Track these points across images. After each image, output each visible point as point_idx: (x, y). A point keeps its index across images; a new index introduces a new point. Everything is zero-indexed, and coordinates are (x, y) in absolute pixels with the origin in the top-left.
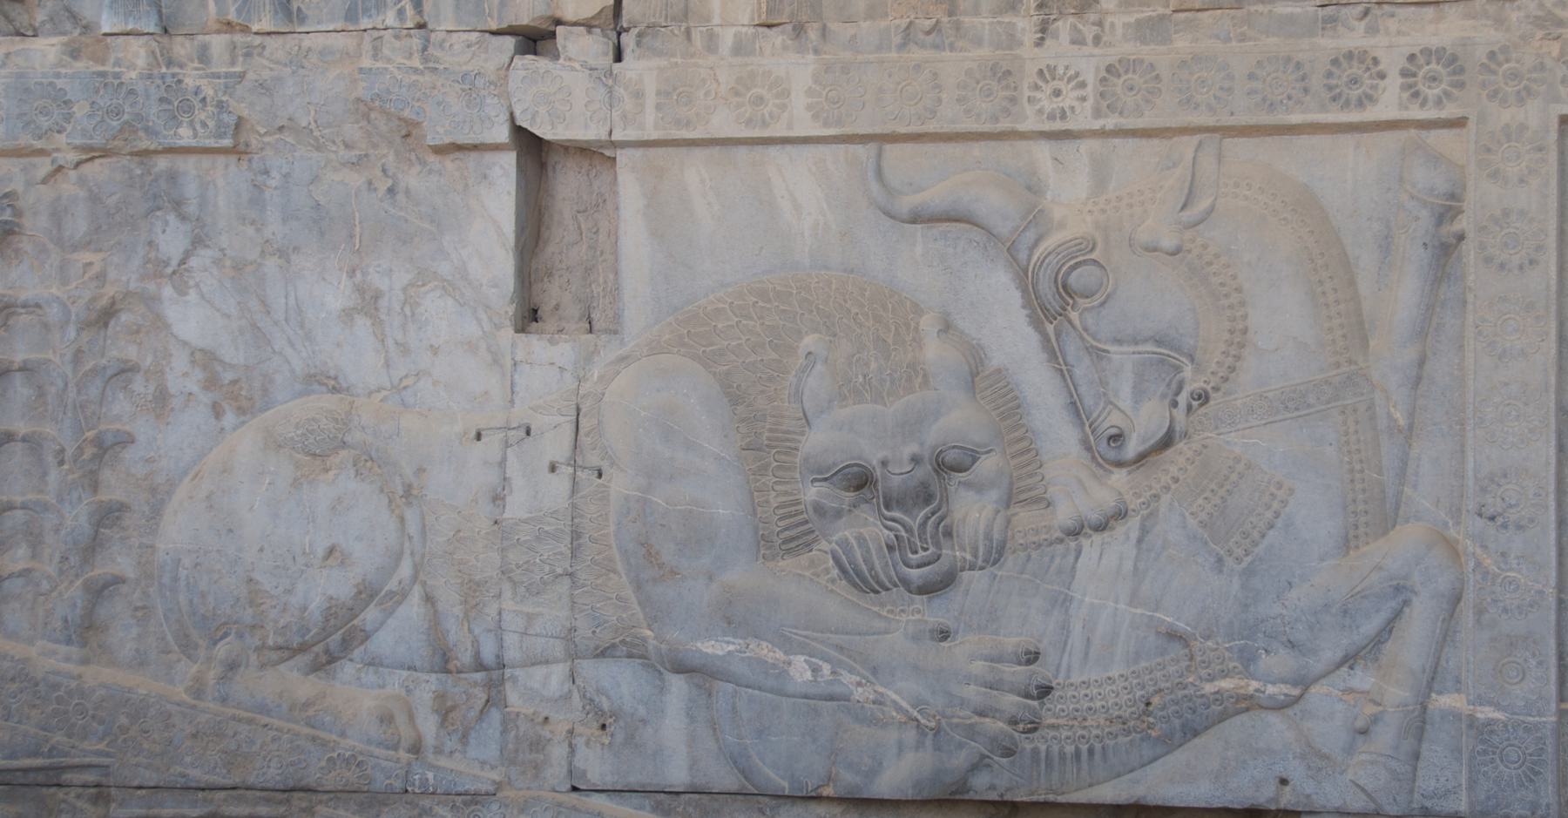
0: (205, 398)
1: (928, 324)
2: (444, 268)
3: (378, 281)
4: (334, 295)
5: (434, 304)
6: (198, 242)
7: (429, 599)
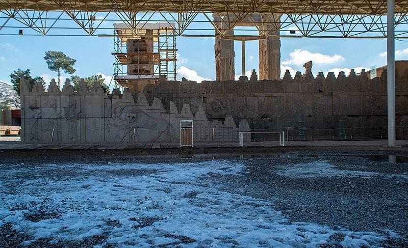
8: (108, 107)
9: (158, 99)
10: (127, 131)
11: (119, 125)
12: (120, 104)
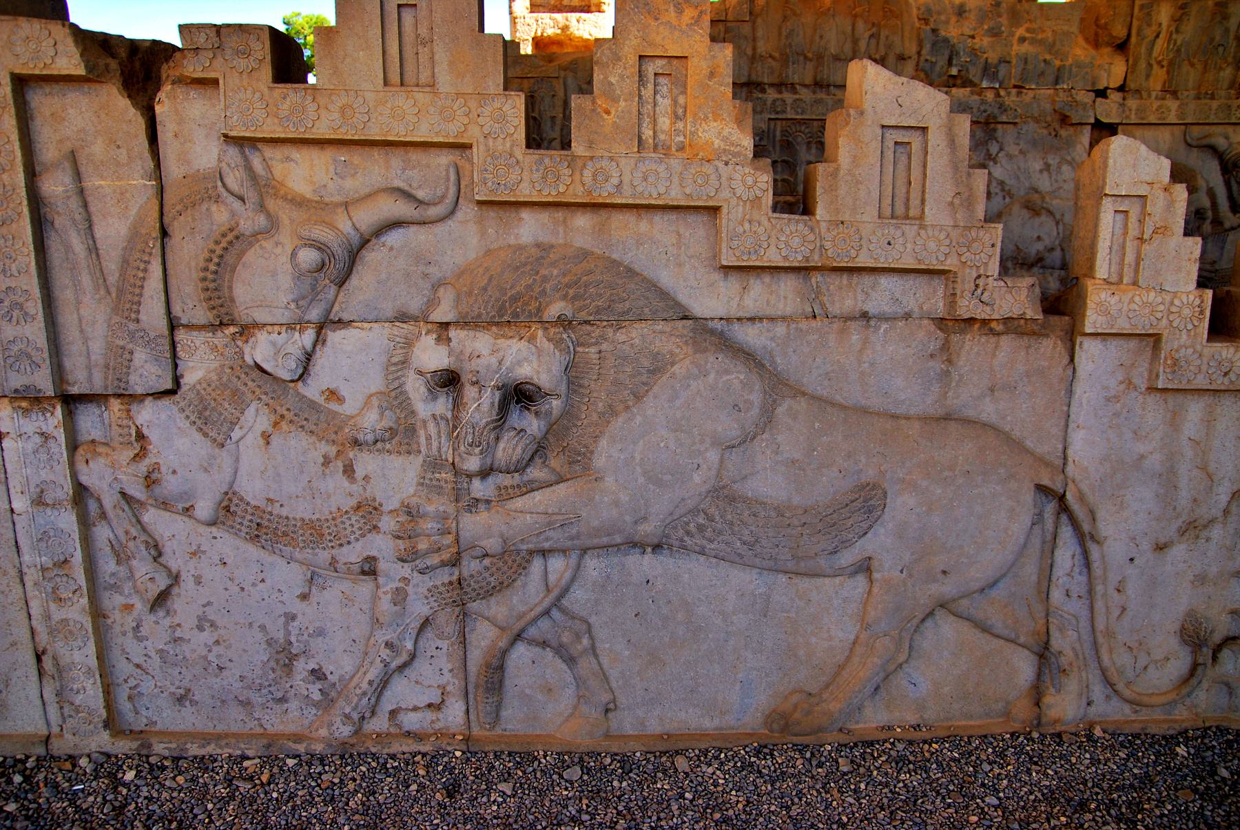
0: (1001, 194)
1: (1199, 177)
2: (1069, 158)
3: (1050, 161)
4: (1038, 165)
5: (1065, 168)
6: (1001, 149)
7: (1063, 250)
8: (113, 230)
9: (927, 103)
10: (419, 608)
11: (301, 510)
12: (303, 173)
